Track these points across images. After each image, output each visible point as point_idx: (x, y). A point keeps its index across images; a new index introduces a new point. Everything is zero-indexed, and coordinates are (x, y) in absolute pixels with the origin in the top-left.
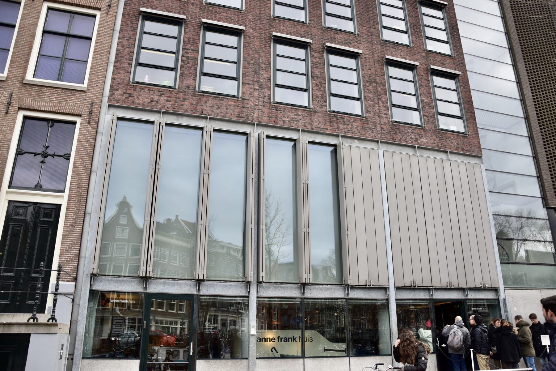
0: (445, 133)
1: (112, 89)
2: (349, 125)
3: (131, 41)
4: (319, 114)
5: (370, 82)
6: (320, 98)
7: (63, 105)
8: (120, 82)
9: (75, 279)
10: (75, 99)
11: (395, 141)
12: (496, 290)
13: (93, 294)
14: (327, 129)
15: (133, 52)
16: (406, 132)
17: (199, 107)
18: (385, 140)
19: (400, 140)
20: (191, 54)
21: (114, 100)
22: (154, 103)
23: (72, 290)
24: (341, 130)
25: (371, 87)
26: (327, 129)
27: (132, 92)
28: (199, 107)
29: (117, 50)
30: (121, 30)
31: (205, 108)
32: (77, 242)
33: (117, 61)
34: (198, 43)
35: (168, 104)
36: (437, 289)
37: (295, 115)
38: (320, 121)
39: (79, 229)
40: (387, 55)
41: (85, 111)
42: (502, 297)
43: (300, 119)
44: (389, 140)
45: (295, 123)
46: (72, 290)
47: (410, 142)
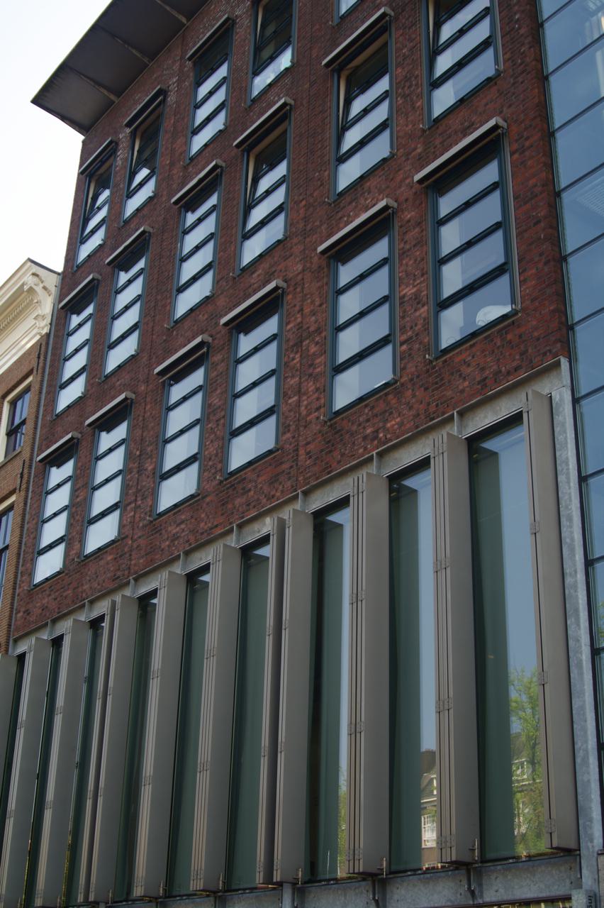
0: (450, 358)
2: (250, 490)
4: (208, 499)
6: (213, 458)
11: (329, 473)
14: (216, 526)
16: (355, 428)
18: (309, 483)
19: (339, 462)
24: (238, 510)
26: (216, 526)
28: (80, 590)
37: (178, 525)
38: (208, 514)
43: (183, 530)
44: (317, 479)
45: (176, 542)
47: (361, 451)
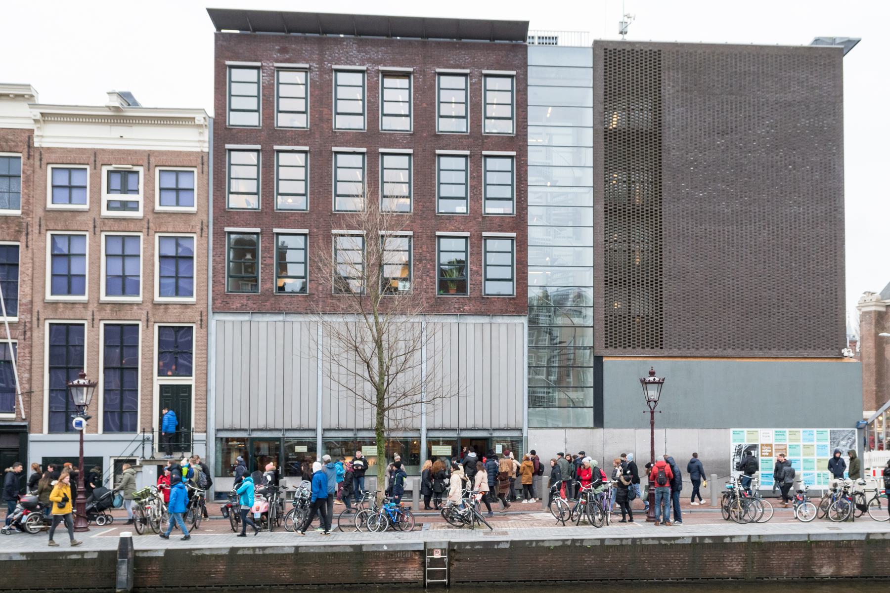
1: (214, 300)
3: (222, 257)
5: (420, 261)
7: (182, 316)
8: (219, 293)
9: (206, 432)
10: (189, 311)
12: (521, 430)
13: (216, 438)
15: (224, 267)
17: (277, 306)
20: (268, 261)
21: (216, 308)
22: (244, 307)
23: (204, 439)
25: (420, 265)
27: (227, 300)
29: (213, 266)
30: (214, 249)
31: (281, 305)
32: (204, 409)
33: (214, 276)
34: (273, 250)
35: (255, 306)
36: (462, 430)
39: (204, 401)
40: (439, 230)
41: (198, 319)
42: (525, 435)
46: (204, 439)
